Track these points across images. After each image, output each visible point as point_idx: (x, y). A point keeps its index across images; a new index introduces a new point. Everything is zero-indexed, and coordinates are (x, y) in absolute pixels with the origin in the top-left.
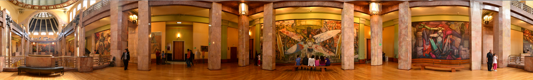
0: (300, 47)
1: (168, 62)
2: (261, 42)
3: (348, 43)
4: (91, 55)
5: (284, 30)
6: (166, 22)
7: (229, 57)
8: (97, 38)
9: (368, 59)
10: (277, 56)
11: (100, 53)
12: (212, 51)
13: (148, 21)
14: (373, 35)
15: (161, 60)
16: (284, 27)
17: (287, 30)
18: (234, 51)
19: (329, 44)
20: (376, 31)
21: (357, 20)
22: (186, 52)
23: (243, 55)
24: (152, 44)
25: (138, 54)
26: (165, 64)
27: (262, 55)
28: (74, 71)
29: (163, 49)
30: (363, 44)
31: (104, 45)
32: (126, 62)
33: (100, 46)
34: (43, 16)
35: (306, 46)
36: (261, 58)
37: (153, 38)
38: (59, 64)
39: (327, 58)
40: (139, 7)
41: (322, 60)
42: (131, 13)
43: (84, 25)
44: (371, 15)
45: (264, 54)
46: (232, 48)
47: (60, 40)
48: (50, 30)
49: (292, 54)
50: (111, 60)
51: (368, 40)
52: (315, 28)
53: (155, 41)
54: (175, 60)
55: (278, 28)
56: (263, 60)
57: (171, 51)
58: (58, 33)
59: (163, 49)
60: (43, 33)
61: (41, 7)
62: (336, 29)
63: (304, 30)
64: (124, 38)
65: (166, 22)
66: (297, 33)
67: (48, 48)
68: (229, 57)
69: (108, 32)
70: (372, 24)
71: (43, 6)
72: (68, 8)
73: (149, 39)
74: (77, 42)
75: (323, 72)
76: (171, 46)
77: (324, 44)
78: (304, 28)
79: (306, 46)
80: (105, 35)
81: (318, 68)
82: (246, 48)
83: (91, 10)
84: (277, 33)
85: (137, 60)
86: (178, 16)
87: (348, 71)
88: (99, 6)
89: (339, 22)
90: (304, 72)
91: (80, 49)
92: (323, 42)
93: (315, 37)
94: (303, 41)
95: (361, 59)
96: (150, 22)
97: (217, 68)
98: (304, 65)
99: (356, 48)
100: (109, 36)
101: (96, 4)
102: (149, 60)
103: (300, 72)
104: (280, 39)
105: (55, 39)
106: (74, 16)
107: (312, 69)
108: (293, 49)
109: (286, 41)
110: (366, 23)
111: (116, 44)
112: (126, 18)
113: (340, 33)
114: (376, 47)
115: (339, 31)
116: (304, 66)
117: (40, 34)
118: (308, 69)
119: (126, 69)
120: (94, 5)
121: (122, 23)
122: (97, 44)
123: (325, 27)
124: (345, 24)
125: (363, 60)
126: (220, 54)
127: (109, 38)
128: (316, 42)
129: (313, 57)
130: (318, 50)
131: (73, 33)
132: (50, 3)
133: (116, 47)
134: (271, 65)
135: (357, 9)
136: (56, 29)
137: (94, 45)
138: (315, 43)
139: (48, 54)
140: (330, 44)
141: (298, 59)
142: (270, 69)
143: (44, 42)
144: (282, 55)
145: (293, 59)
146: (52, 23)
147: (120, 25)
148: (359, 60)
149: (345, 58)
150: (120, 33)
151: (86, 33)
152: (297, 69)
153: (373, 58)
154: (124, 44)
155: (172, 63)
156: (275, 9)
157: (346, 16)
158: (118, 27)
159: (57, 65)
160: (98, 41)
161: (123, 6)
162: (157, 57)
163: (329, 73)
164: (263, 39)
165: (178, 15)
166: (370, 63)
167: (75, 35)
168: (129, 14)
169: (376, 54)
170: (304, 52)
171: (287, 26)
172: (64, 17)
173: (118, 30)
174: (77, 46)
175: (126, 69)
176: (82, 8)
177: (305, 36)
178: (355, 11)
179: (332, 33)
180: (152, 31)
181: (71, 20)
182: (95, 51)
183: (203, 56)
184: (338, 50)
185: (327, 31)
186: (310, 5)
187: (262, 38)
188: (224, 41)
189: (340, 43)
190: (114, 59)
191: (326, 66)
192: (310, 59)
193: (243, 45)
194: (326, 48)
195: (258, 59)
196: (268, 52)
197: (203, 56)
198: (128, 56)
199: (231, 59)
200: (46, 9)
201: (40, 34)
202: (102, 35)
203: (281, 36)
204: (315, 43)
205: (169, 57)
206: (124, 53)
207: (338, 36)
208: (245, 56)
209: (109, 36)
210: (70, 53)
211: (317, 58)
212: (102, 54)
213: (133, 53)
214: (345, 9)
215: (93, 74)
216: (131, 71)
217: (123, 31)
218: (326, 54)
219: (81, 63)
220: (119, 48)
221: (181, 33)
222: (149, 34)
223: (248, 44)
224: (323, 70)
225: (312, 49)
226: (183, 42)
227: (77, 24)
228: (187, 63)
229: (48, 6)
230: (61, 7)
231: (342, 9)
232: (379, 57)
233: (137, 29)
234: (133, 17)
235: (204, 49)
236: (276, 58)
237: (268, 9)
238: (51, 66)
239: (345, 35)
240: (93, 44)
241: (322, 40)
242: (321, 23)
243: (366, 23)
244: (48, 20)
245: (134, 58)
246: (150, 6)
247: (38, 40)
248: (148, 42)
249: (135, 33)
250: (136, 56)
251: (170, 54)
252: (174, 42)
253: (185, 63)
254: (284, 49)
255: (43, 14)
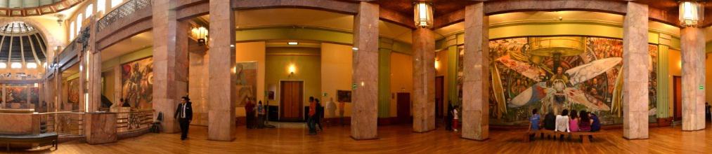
0: (539, 93)
1: (271, 123)
2: (460, 83)
3: (637, 85)
4: (112, 110)
5: (507, 58)
6: (266, 41)
7: (394, 114)
8: (125, 74)
9: (675, 120)
10: (491, 111)
11: (132, 105)
12: (359, 102)
13: (229, 40)
14: (687, 68)
15: (255, 119)
16: (505, 53)
17: (512, 58)
18: (404, 101)
19: (599, 87)
20: (692, 60)
21: (654, 38)
22: (306, 103)
23: (423, 110)
24: (238, 88)
25: (209, 107)
26: (264, 127)
27: (461, 109)
28: (80, 141)
29: (261, 96)
30: (668, 88)
31: (140, 89)
32: (185, 122)
33: (132, 91)
34: (16, 31)
35: (550, 92)
36: (460, 115)
37: (239, 74)
38: (49, 128)
39: (594, 116)
40: (211, 10)
41: (584, 120)
42: (194, 23)
43: (98, 48)
44: (682, 28)
45: (466, 107)
46: (400, 95)
47: (51, 79)
48: (29, 57)
49: (523, 107)
50: (155, 119)
51: (677, 79)
52: (569, 54)
53: (243, 80)
54: (283, 120)
55: (493, 54)
56: (464, 120)
57: (276, 102)
58: (45, 64)
59: (261, 96)
60: (16, 65)
61: (12, 10)
62: (611, 56)
63: (546, 58)
64: (180, 74)
65: (266, 41)
66: (532, 64)
67: (26, 95)
68: (394, 114)
69: (147, 62)
70: (683, 45)
71: (16, 9)
72: (67, 14)
73: (232, 76)
74: (85, 82)
75: (586, 143)
76: (277, 91)
77: (588, 87)
78: (546, 54)
79: (550, 92)
80: (141, 69)
81: (576, 135)
82: (429, 94)
83: (114, 18)
84: (492, 65)
85: (207, 118)
86: (290, 30)
87: (637, 142)
88: (130, 9)
89: (618, 42)
90: (547, 143)
91: (91, 97)
92: (586, 82)
93: (570, 72)
94: (544, 80)
95: (661, 116)
96: (233, 41)
97: (370, 137)
98: (548, 128)
99: (652, 94)
100: (150, 70)
101: (123, 5)
102: (232, 119)
103: (539, 143)
104: (497, 76)
105: (39, 77)
106: (79, 30)
107: (562, 138)
108: (525, 96)
109: (511, 80)
110: (673, 43)
111: (164, 86)
112: (184, 33)
113: (620, 65)
114: (693, 93)
115: (619, 60)
116: (546, 132)
117: (9, 67)
118: (555, 138)
119: (184, 137)
120: (119, 8)
121: (177, 44)
122: (126, 86)
123: (589, 53)
124: (631, 47)
125: (666, 120)
126: (376, 107)
127: (151, 75)
128: (572, 82)
129: (564, 113)
130: (576, 99)
131: (77, 64)
132: (30, 1)
133: (165, 94)
134: (480, 129)
135: (655, 16)
136: (42, 57)
137: (119, 89)
138: (569, 85)
139: (26, 107)
140: (599, 86)
141: (535, 117)
142: (477, 137)
143: (16, 83)
144: (502, 108)
145: (525, 117)
146: (33, 45)
147: (173, 49)
148: (658, 120)
149: (631, 115)
150: (173, 64)
151: (103, 63)
152: (532, 138)
153: (685, 116)
154: (180, 86)
155: (278, 125)
156: (487, 14)
157: (632, 29)
158: (169, 51)
159: (43, 129)
160: (128, 81)
161: (178, 9)
162: (247, 113)
163: (597, 145)
164: (464, 77)
165: (290, 27)
166: (681, 125)
167: (81, 68)
168: (191, 26)
169: (693, 108)
170: (547, 104)
171: (512, 49)
172: (57, 31)
173: (169, 58)
174: (85, 91)
175: (184, 137)
176: (96, 14)
177: (549, 71)
178: (651, 19)
179: (604, 65)
180: (238, 61)
181: (72, 38)
182: (122, 100)
183: (342, 112)
184: (617, 100)
185: (593, 59)
186: (559, 7)
187: (461, 74)
188: (383, 80)
189: (621, 85)
190: (160, 117)
191: (592, 131)
192: (559, 117)
193: (422, 88)
194: (592, 94)
195: (453, 117)
196: (473, 103)
197: (342, 112)
198: (189, 112)
199: (398, 118)
200: (22, 15)
201: (9, 67)
202: (136, 68)
203: (500, 70)
204: (569, 85)
205: (272, 113)
206: (180, 105)
207: (615, 71)
208: (426, 112)
209: (150, 70)
210: (71, 105)
211: (573, 115)
212: (136, 106)
213: (198, 105)
214: (630, 15)
215: (118, 148)
216: (193, 140)
217: (178, 60)
218: (592, 107)
219: (92, 125)
220: (171, 94)
221: (297, 65)
222: (232, 66)
223: (433, 87)
224: (586, 139)
225: (564, 97)
226: (301, 83)
227: (85, 47)
228: (309, 125)
229: (26, 9)
230: (52, 12)
231: (624, 14)
232: (698, 113)
233: (207, 57)
234: (199, 32)
235: (344, 96)
236: (491, 115)
237: (474, 13)
238: (31, 132)
239: (631, 67)
240: (118, 86)
241: (584, 79)
242: (582, 44)
243: (673, 43)
244: (25, 38)
245: (200, 114)
246: (233, 10)
247: (6, 78)
248: (228, 81)
249: (202, 64)
250: (204, 111)
251: (275, 108)
252: (283, 83)
253: (304, 126)
254: (507, 97)
255: (16, 25)
